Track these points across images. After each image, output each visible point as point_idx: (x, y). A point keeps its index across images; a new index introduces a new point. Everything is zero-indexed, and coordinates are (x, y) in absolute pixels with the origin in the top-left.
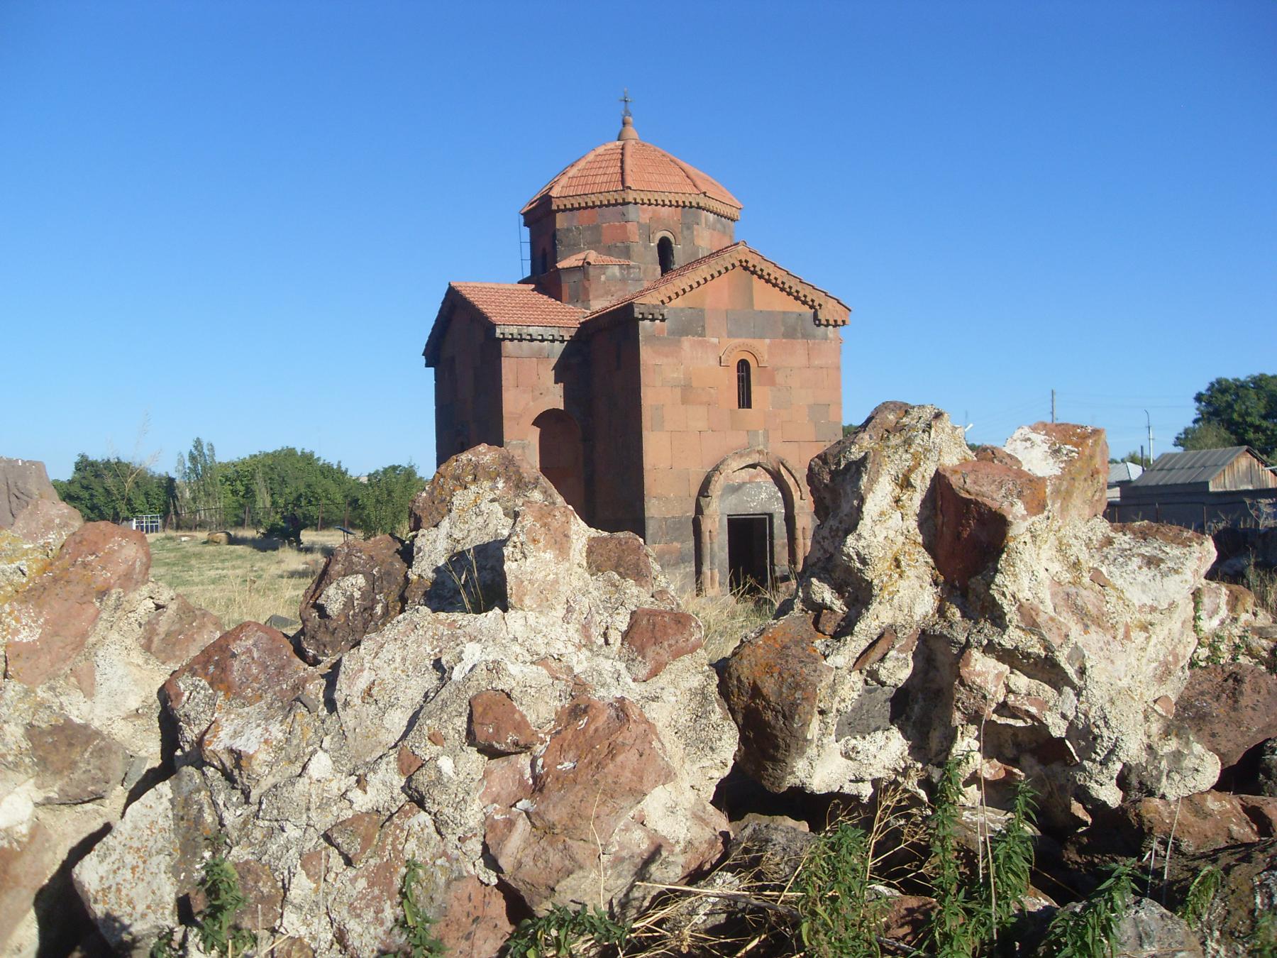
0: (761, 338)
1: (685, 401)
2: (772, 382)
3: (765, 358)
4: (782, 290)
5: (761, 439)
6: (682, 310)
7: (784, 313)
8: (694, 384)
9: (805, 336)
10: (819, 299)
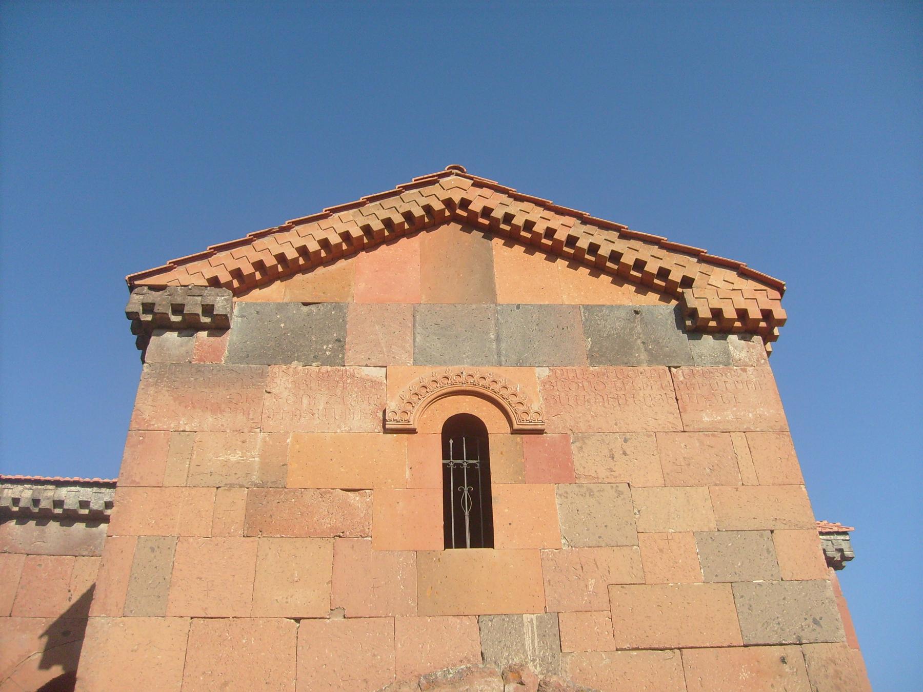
0: (520, 363)
1: (256, 526)
2: (563, 471)
3: (534, 405)
4: (576, 261)
5: (530, 640)
6: (281, 307)
7: (587, 307)
8: (294, 480)
9: (653, 359)
10: (679, 267)
